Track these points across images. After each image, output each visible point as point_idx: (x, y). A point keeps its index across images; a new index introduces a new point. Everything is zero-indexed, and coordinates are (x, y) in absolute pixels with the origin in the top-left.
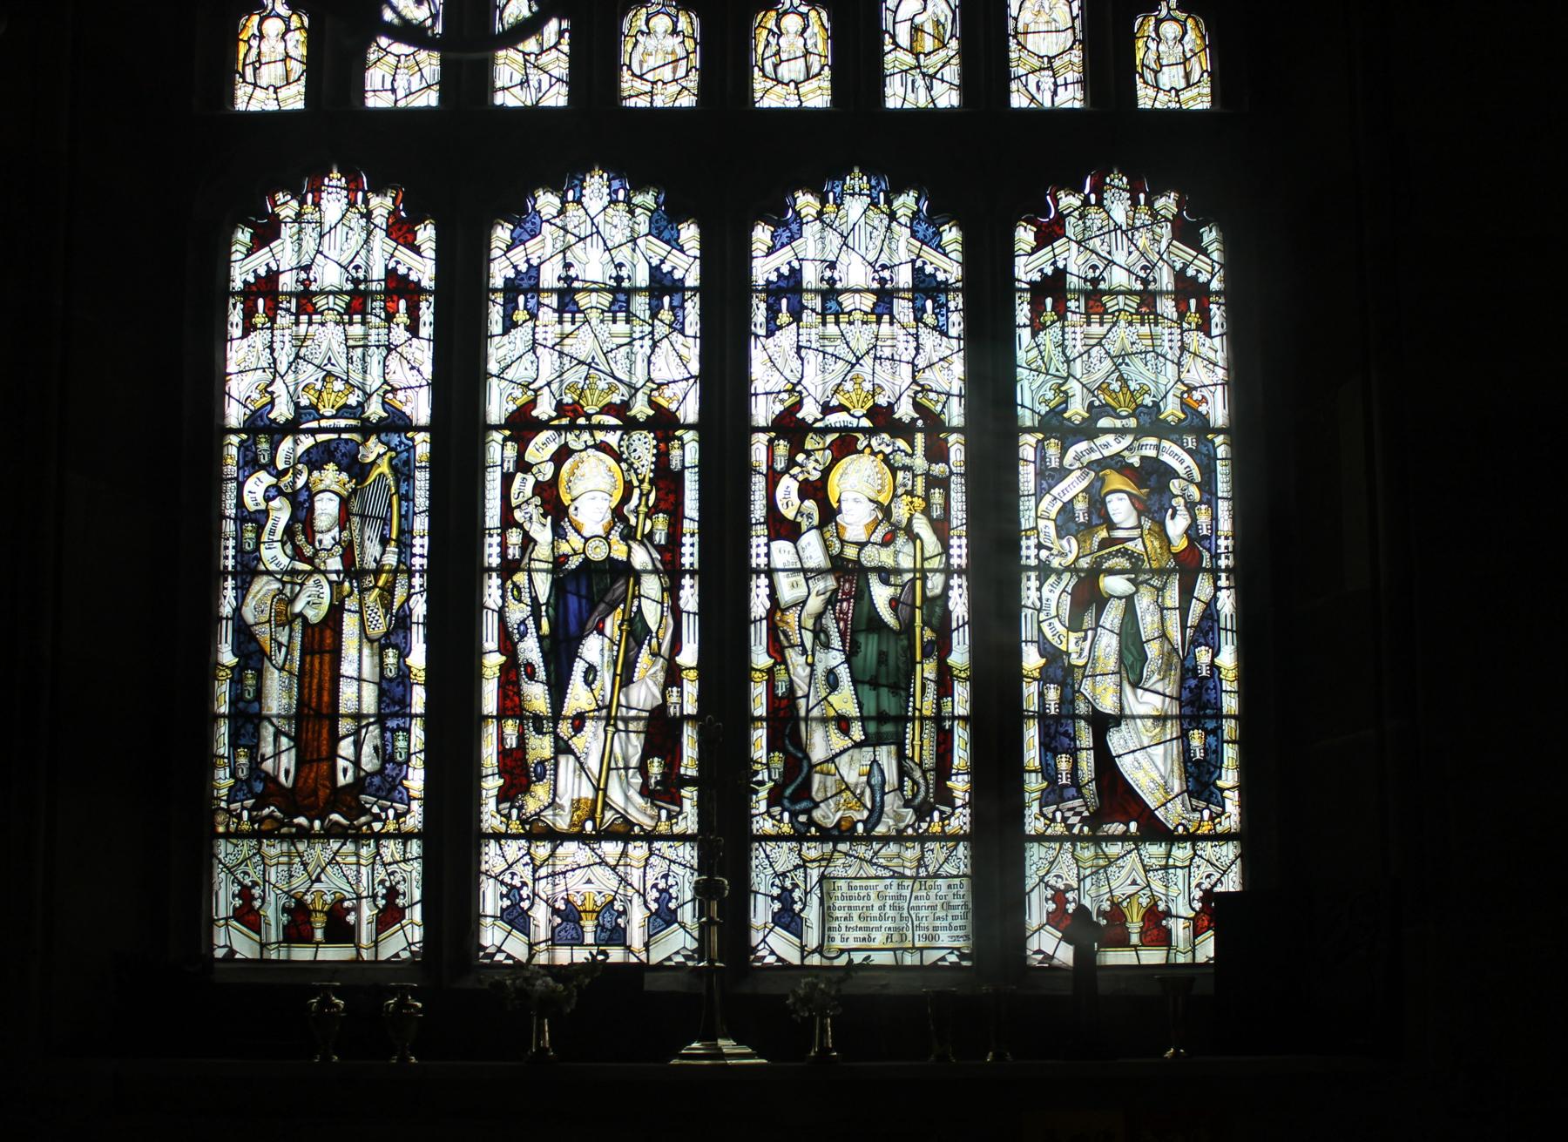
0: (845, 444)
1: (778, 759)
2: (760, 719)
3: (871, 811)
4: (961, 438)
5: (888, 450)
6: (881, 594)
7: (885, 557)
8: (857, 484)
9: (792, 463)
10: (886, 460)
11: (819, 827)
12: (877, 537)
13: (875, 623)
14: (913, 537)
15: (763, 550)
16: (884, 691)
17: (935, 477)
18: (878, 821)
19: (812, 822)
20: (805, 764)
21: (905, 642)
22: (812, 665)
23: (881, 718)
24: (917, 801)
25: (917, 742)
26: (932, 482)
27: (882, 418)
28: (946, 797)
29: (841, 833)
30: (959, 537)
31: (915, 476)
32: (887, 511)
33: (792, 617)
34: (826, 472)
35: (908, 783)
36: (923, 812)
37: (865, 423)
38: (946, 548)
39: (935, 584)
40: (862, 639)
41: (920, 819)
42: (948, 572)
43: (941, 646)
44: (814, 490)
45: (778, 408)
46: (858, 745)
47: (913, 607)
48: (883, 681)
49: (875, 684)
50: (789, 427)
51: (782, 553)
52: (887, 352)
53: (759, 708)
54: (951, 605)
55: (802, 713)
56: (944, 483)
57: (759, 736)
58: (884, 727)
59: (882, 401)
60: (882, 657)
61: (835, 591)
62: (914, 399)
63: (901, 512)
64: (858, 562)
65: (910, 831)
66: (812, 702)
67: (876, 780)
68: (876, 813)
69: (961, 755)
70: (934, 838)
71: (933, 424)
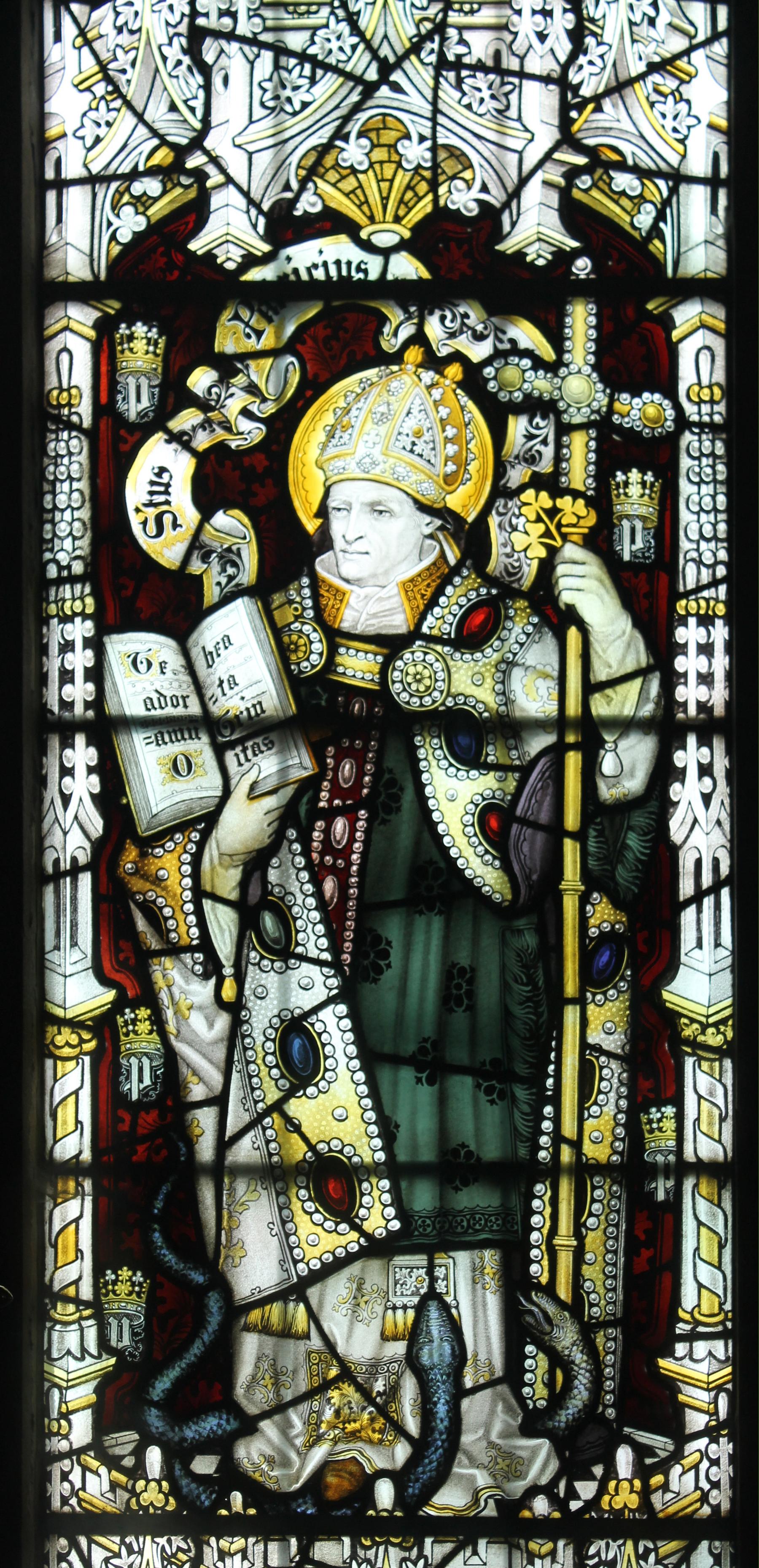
0: (341, 333)
1: (127, 1287)
2: (73, 1168)
3: (419, 1446)
4: (716, 315)
5: (478, 352)
6: (454, 794)
7: (470, 681)
8: (380, 462)
9: (173, 395)
10: (473, 381)
11: (254, 1491)
12: (442, 619)
13: (435, 881)
14: (559, 619)
15: (81, 660)
16: (462, 1087)
17: (630, 434)
18: (441, 1477)
19: (231, 1476)
20: (214, 1303)
21: (530, 940)
22: (235, 1009)
23: (454, 1166)
24: (564, 1417)
25: (565, 1239)
26: (619, 448)
27: (463, 256)
28: (655, 1404)
29: (331, 1508)
30: (706, 621)
31: (563, 429)
32: (473, 538)
33: (171, 864)
34: (283, 425)
35: (536, 1364)
36: (583, 1448)
37: (406, 267)
38: (662, 652)
39: (627, 764)
40: (392, 929)
41: (573, 1467)
42: (668, 727)
43: (646, 949)
44: (242, 473)
45: (130, 224)
46: (378, 1249)
47: (556, 831)
48: (459, 1054)
49: (433, 1064)
50: (166, 284)
51: (142, 671)
52: (481, 46)
53: (72, 1137)
54: (677, 829)
55: (206, 1150)
56: (657, 455)
57: (73, 1217)
58: (463, 1194)
59: (462, 199)
60: (457, 986)
61: (309, 786)
62: (565, 193)
63: (518, 542)
64: (381, 694)
65: (541, 1506)
66: (236, 1118)
67: (436, 1352)
68: (435, 1451)
69: (704, 1279)
70: (618, 1527)
71: (625, 280)
